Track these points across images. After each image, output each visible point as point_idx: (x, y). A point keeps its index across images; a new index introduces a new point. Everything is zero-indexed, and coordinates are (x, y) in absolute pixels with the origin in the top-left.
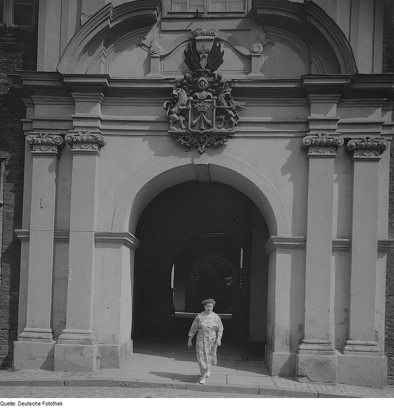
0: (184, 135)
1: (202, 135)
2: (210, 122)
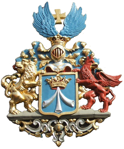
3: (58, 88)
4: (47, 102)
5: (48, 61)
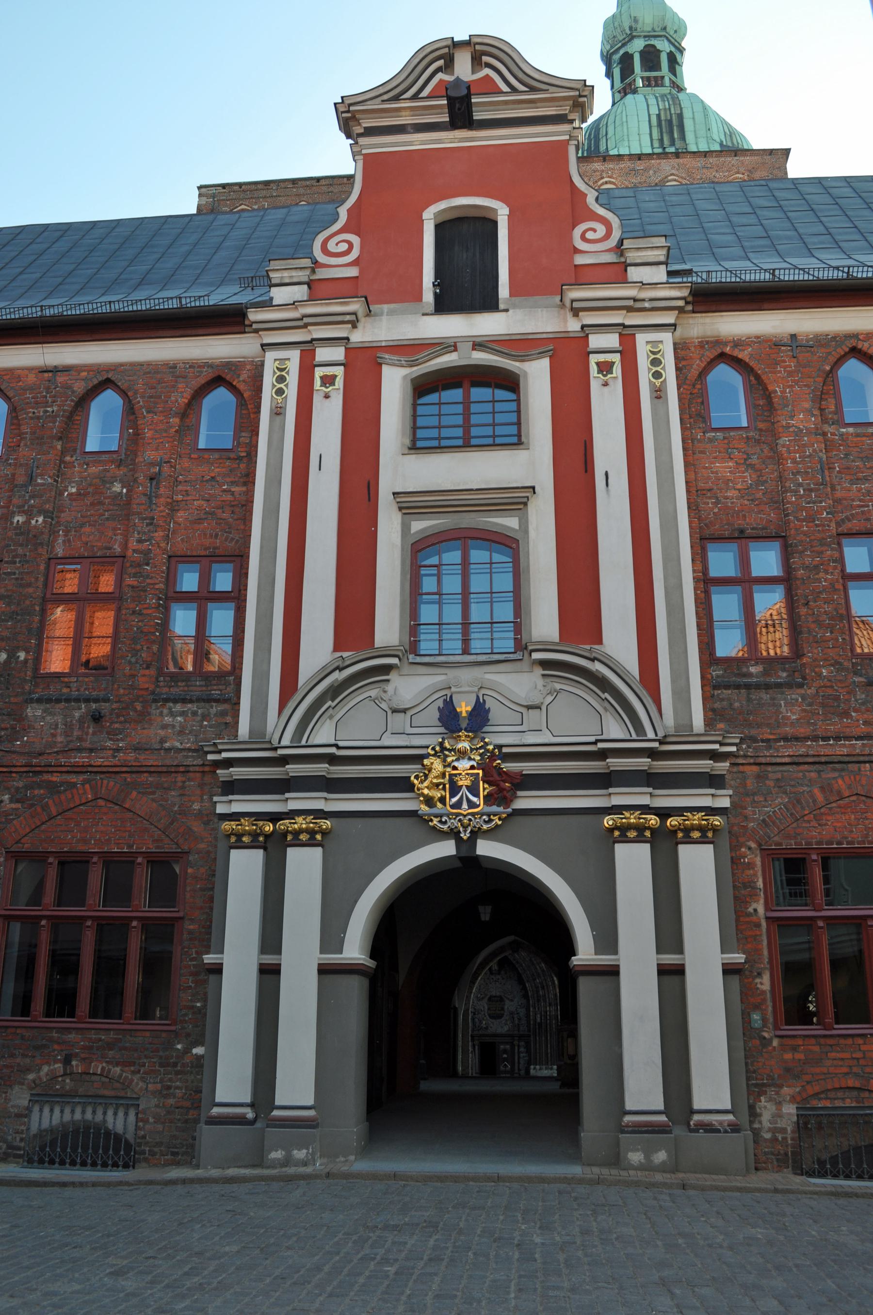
0: (441, 817)
1: (465, 816)
2: (474, 799)
3: (464, 787)
4: (454, 800)
5: (454, 758)
